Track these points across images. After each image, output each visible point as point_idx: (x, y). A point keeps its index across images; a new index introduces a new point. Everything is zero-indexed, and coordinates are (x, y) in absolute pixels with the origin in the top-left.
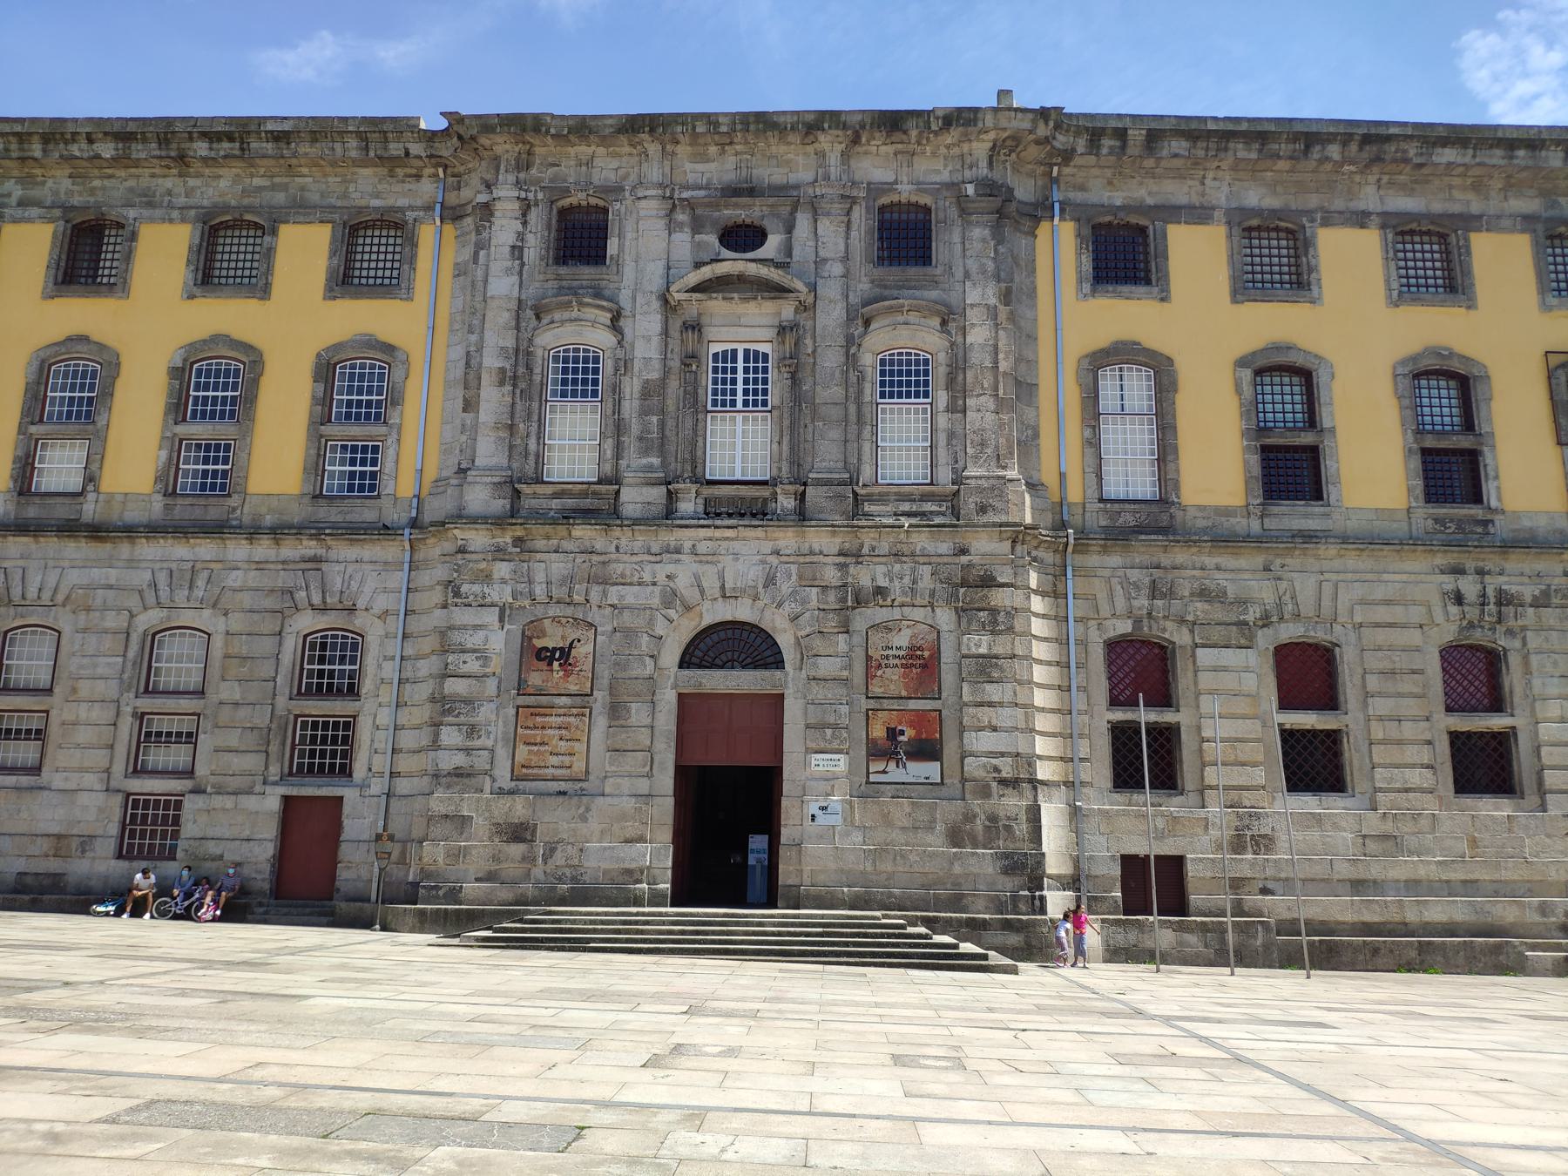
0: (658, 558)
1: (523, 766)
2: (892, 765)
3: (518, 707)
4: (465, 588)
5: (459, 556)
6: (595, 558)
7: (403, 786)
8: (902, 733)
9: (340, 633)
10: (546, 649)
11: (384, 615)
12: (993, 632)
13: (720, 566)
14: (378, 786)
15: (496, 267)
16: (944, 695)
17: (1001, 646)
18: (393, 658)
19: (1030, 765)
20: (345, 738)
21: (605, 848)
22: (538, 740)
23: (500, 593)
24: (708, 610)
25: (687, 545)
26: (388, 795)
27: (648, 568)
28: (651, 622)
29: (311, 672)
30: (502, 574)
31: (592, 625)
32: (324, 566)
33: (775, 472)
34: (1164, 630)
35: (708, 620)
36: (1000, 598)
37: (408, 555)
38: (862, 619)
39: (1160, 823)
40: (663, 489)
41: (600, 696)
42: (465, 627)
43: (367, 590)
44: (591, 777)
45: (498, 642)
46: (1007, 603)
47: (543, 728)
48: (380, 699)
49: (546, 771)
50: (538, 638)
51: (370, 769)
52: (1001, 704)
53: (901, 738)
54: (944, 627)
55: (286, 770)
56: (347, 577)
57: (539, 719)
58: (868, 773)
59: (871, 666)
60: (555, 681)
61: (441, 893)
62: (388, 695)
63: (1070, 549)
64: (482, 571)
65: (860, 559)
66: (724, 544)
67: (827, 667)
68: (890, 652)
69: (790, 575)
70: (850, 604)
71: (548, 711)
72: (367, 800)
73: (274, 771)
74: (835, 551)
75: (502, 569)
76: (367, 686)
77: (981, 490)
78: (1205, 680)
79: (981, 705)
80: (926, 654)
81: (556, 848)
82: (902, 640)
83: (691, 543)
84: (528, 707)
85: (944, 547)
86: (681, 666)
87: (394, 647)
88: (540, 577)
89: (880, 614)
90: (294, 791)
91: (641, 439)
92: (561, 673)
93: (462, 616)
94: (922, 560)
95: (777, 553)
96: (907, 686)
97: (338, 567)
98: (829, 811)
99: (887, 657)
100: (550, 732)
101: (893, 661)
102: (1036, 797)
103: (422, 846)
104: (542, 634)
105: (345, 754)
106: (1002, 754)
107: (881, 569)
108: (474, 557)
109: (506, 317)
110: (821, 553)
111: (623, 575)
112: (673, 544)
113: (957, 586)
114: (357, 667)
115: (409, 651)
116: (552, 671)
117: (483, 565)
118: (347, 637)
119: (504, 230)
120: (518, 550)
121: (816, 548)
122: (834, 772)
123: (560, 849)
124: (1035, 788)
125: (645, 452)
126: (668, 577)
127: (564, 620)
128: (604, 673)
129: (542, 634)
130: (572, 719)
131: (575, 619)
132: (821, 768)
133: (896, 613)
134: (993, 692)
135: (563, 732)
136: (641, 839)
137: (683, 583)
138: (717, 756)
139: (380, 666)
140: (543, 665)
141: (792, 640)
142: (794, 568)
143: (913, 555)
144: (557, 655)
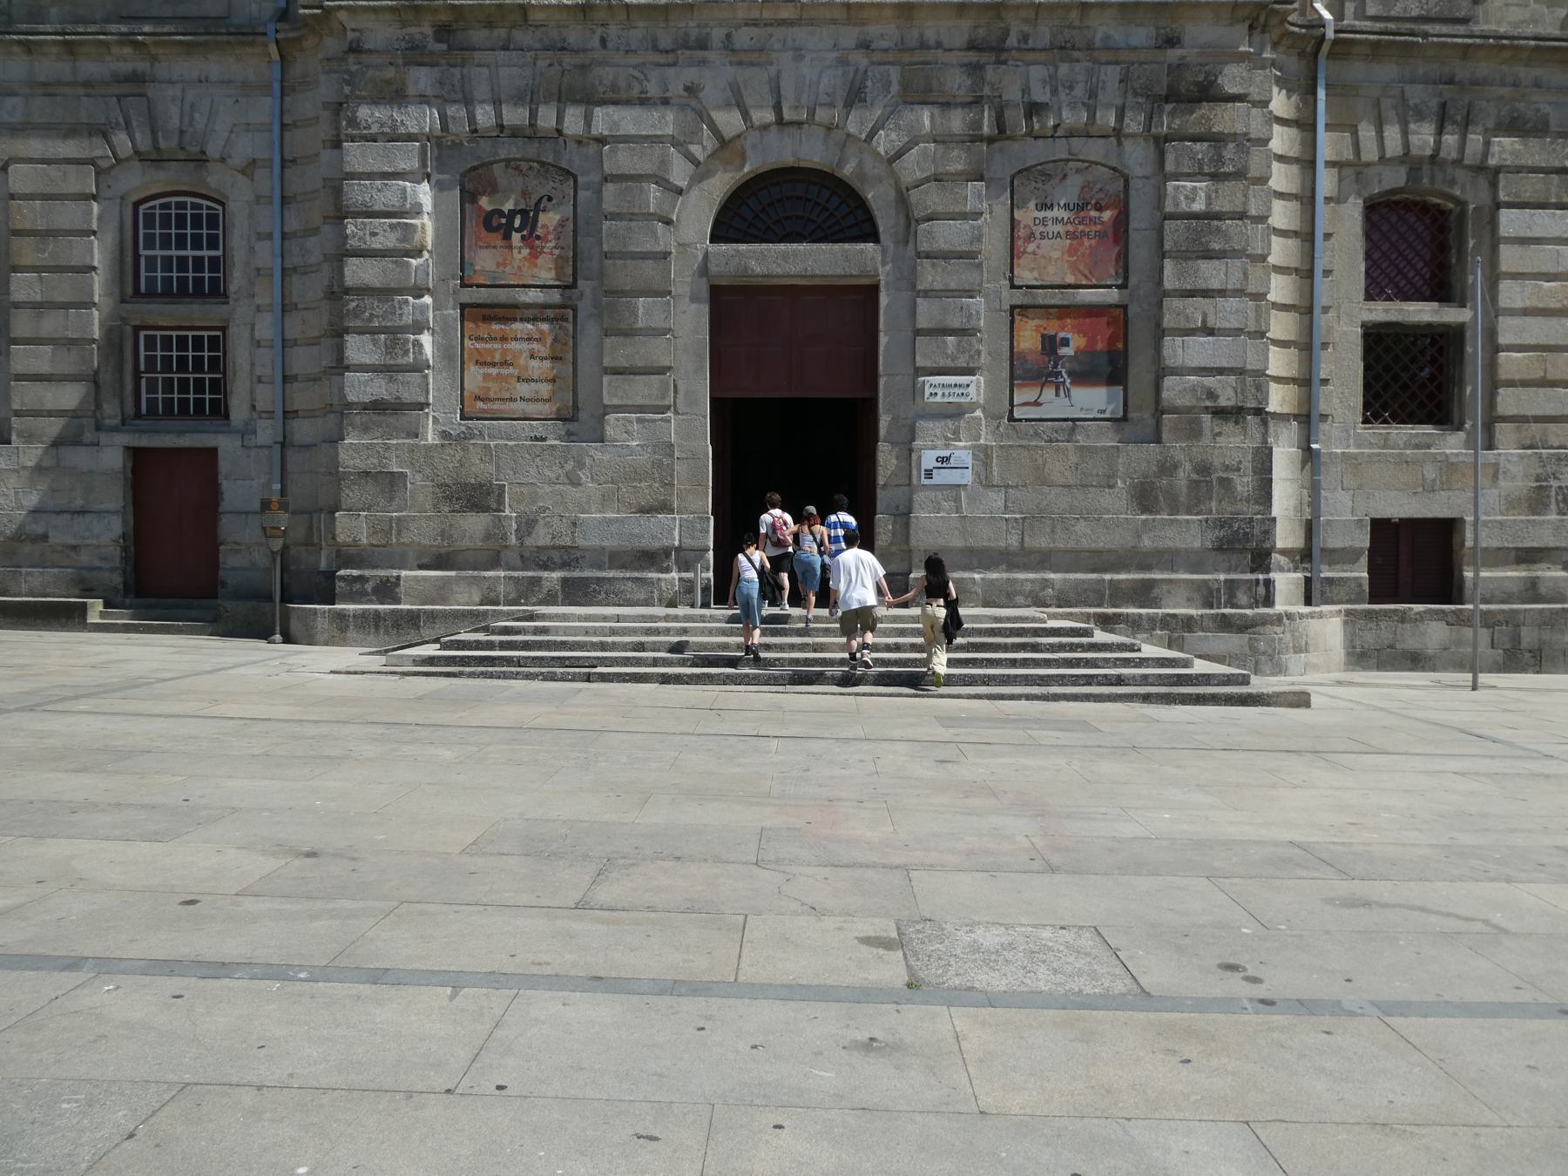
0: (671, 58)
1: (478, 398)
2: (1049, 393)
5: (351, 58)
6: (569, 60)
7: (304, 430)
8: (1065, 342)
9: (189, 200)
11: (249, 168)
12: (1215, 177)
13: (773, 70)
14: (266, 432)
17: (1228, 198)
18: (270, 236)
19: (1258, 387)
20: (214, 362)
21: (610, 522)
22: (498, 358)
24: (754, 147)
25: (717, 34)
26: (283, 445)
27: (654, 74)
28: (664, 163)
29: (151, 261)
30: (421, 86)
31: (568, 173)
32: (151, 90)
34: (1453, 182)
36: (1226, 119)
37: (277, 68)
39: (1430, 472)
42: (370, 176)
44: (583, 415)
46: (1240, 128)
47: (504, 339)
48: (258, 301)
49: (513, 406)
51: (254, 407)
52: (1222, 293)
53: (1064, 351)
55: (130, 408)
56: (187, 107)
57: (495, 327)
58: (1012, 404)
60: (516, 264)
61: (369, 587)
62: (268, 294)
63: (1325, 48)
64: (389, 82)
65: (1004, 57)
66: (779, 32)
68: (1049, 214)
69: (889, 84)
70: (986, 130)
71: (509, 313)
72: (253, 453)
73: (110, 409)
74: (960, 40)
75: (421, 79)
76: (237, 281)
78: (1509, 258)
79: (1191, 294)
81: (535, 521)
83: (722, 32)
84: (478, 306)
85: (1141, 35)
86: (715, 238)
87: (268, 219)
90: (144, 441)
92: (526, 252)
94: (1104, 57)
95: (865, 45)
96: (1074, 268)
97: (173, 91)
98: (953, 463)
99: (1044, 221)
100: (514, 345)
101: (1059, 228)
102: (1265, 435)
103: (334, 519)
105: (216, 386)
106: (1220, 371)
107: (1037, 73)
108: (375, 59)
110: (939, 45)
111: (614, 87)
112: (694, 33)
115: (293, 224)
116: (510, 247)
117: (390, 73)
118: (200, 207)
120: (444, 47)
121: (931, 36)
122: (959, 405)
123: (541, 522)
124: (1265, 423)
126: (687, 89)
127: (524, 166)
131: (543, 164)
132: (938, 399)
133: (1059, 149)
134: (1211, 273)
135: (535, 346)
136: (665, 507)
138: (775, 384)
139: (252, 250)
140: (496, 238)
141: (892, 194)
142: (894, 73)
143: (1090, 47)
144: (517, 223)
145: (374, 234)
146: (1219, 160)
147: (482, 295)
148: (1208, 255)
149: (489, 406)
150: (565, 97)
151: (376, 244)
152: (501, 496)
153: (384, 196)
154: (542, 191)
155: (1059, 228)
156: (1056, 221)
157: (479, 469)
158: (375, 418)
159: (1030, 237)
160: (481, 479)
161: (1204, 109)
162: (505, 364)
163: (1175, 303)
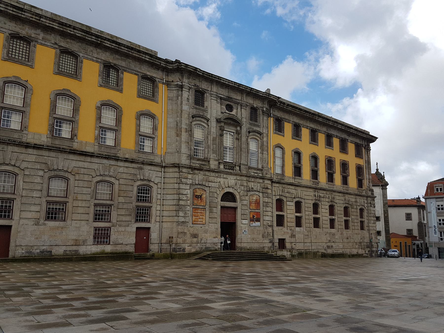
3: (193, 208)
4: (183, 180)
8: (255, 216)
10: (197, 195)
15: (184, 102)
16: (261, 209)
23: (189, 182)
33: (235, 161)
35: (225, 191)
38: (249, 193)
40: (218, 162)
41: (207, 207)
43: (154, 176)
45: (189, 192)
50: (196, 193)
54: (261, 196)
57: (196, 211)
59: (250, 203)
64: (186, 176)
67: (245, 202)
75: (190, 176)
77: (266, 170)
79: (266, 211)
80: (258, 201)
82: (255, 198)
88: (197, 179)
89: (252, 193)
91: (213, 150)
93: (182, 186)
99: (252, 201)
100: (198, 214)
101: (254, 202)
104: (196, 192)
107: (253, 184)
109: (186, 116)
111: (211, 180)
113: (263, 188)
114: (150, 195)
119: (186, 94)
125: (213, 153)
128: (208, 201)
129: (196, 192)
130: (202, 211)
137: (222, 183)
140: (197, 199)
145: (183, 197)
146: (268, 196)
147: (195, 207)
148: (268, 207)
149: (195, 222)
150: (206, 181)
151: (184, 199)
152: (198, 236)
153: (185, 192)
154: (202, 193)
155: (254, 202)
156: (254, 201)
157: (196, 232)
158: (183, 224)
159: (251, 203)
160: (196, 233)
161: (267, 190)
162: (197, 216)
163: (265, 212)
